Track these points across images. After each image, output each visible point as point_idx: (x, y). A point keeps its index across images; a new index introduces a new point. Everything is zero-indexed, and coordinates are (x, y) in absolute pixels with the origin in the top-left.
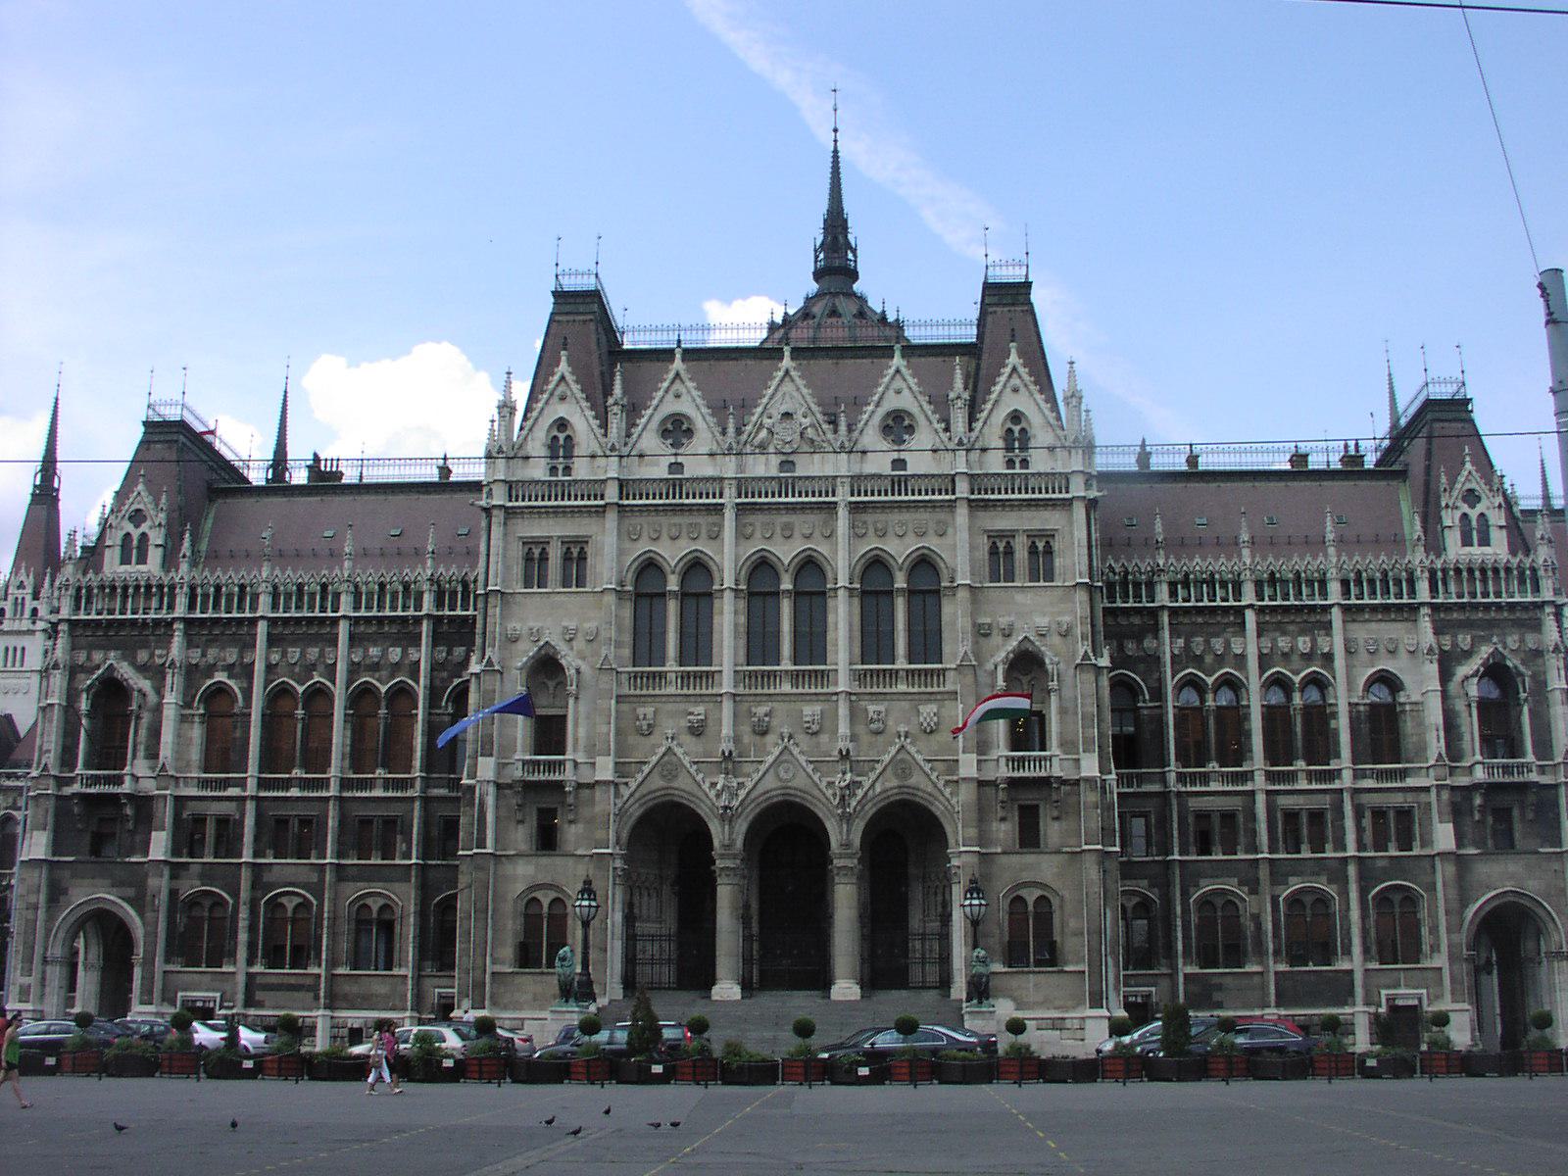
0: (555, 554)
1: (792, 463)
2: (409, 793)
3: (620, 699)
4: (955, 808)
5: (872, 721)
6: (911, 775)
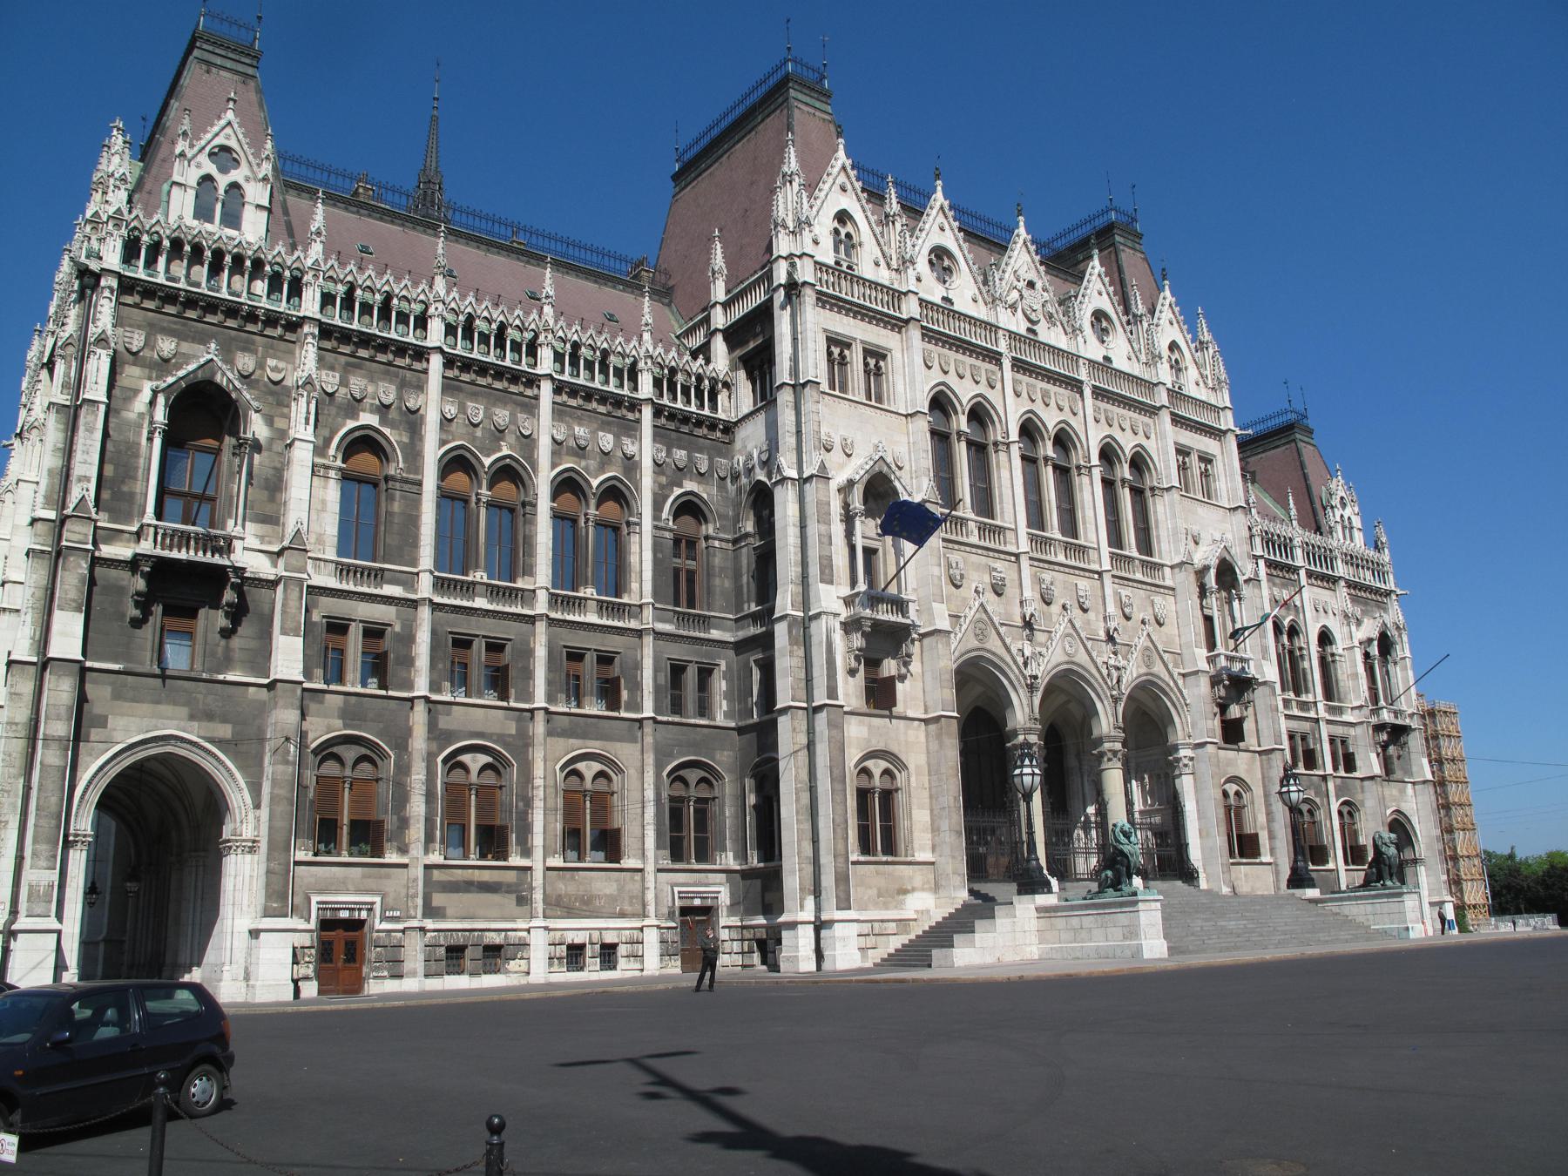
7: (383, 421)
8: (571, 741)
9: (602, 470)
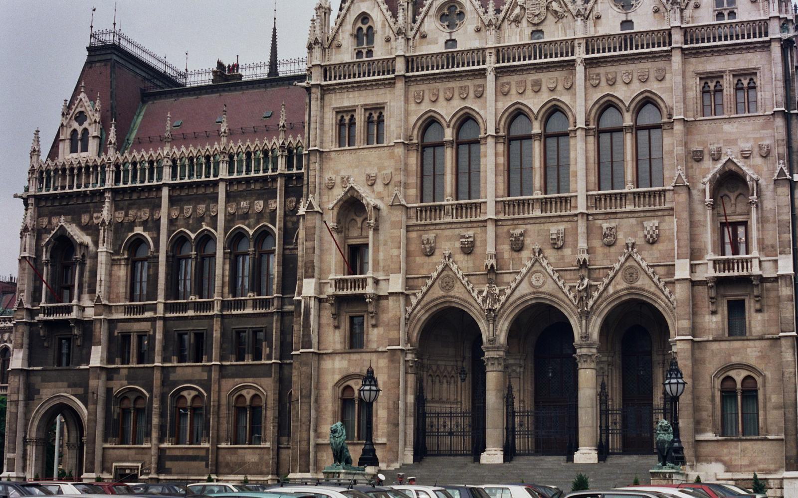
0: (360, 118)
1: (541, 31)
2: (272, 309)
3: (408, 228)
4: (674, 304)
5: (605, 236)
6: (637, 279)
7: (144, 230)
8: (236, 380)
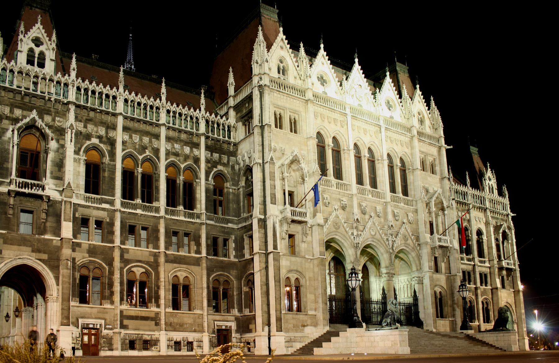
7: (100, 142)
8: (175, 265)
9: (185, 160)
